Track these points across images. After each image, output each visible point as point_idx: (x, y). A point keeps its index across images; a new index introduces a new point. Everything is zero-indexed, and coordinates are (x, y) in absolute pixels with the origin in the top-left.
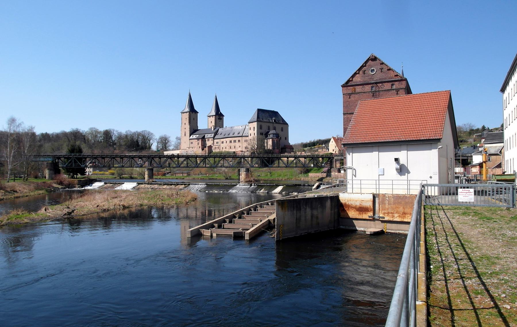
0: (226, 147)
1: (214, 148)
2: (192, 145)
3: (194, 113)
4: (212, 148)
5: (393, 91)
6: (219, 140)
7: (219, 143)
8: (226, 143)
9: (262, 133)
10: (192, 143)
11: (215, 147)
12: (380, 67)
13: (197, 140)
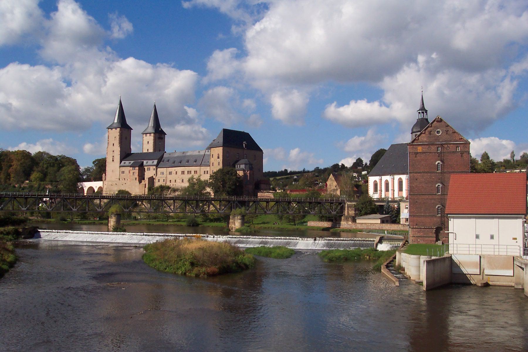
0: (175, 180)
3: (126, 130)
4: (155, 180)
5: (457, 154)
6: (166, 168)
8: (176, 174)
10: (123, 172)
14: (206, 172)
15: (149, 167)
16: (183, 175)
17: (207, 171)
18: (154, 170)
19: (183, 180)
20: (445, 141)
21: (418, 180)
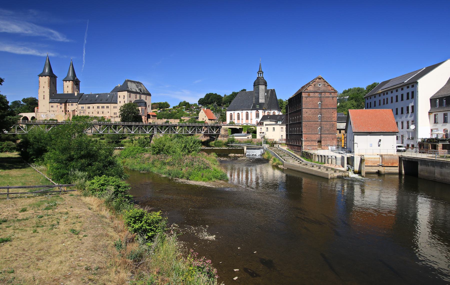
0: (93, 112)
1: (79, 112)
2: (52, 109)
7: (85, 108)
8: (93, 108)
10: (52, 107)
11: (80, 112)
12: (323, 83)
13: (59, 104)
14: (115, 107)
16: (98, 109)
17: (116, 107)
19: (98, 112)
20: (324, 90)
21: (308, 113)
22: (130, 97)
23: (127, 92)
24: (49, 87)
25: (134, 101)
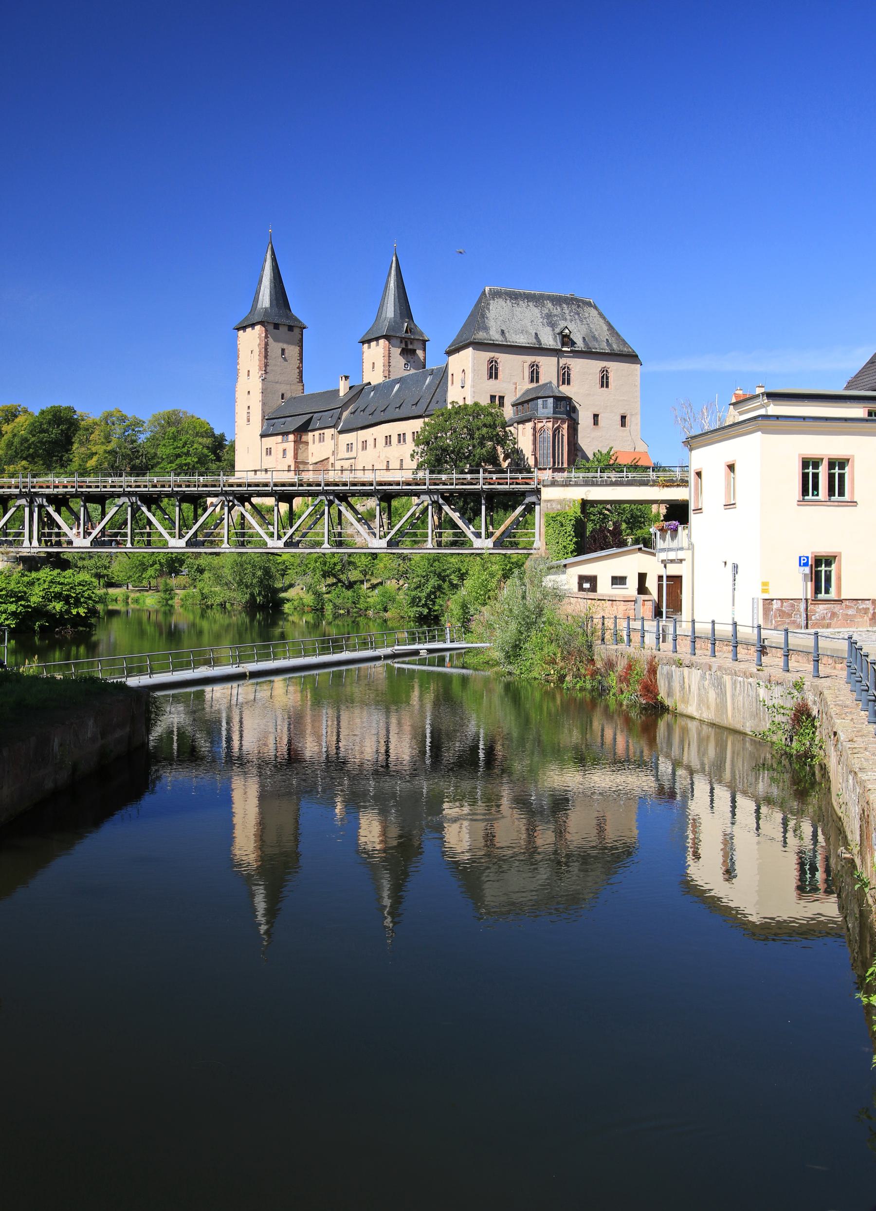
9: (502, 398)
10: (269, 452)
13: (280, 438)
15: (322, 432)
16: (388, 448)
18: (332, 439)
22: (493, 372)
23: (471, 348)
24: (260, 369)
25: (519, 395)
